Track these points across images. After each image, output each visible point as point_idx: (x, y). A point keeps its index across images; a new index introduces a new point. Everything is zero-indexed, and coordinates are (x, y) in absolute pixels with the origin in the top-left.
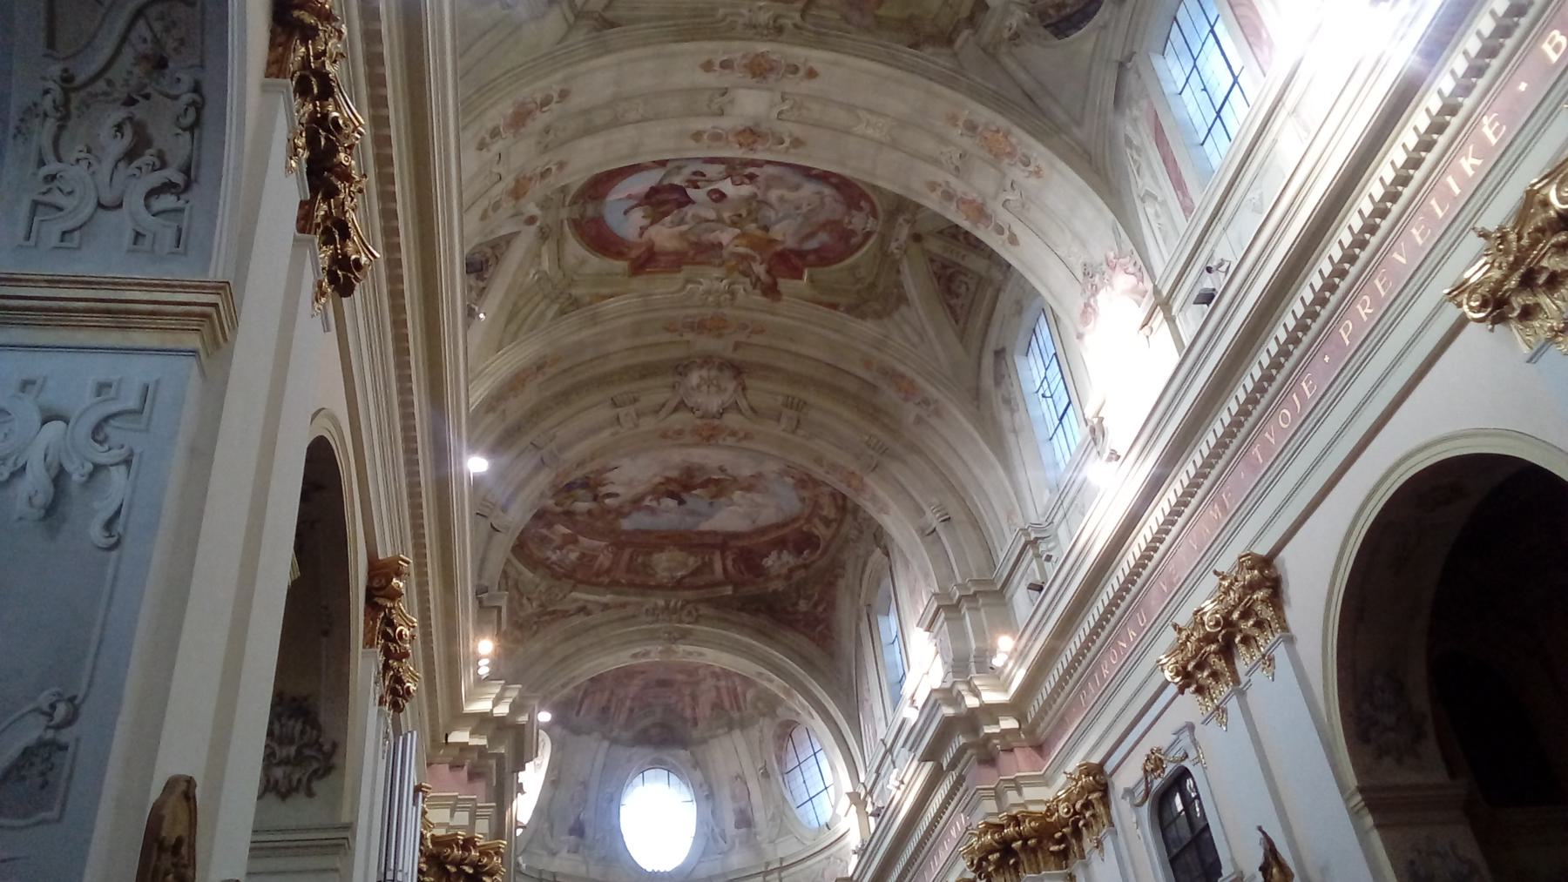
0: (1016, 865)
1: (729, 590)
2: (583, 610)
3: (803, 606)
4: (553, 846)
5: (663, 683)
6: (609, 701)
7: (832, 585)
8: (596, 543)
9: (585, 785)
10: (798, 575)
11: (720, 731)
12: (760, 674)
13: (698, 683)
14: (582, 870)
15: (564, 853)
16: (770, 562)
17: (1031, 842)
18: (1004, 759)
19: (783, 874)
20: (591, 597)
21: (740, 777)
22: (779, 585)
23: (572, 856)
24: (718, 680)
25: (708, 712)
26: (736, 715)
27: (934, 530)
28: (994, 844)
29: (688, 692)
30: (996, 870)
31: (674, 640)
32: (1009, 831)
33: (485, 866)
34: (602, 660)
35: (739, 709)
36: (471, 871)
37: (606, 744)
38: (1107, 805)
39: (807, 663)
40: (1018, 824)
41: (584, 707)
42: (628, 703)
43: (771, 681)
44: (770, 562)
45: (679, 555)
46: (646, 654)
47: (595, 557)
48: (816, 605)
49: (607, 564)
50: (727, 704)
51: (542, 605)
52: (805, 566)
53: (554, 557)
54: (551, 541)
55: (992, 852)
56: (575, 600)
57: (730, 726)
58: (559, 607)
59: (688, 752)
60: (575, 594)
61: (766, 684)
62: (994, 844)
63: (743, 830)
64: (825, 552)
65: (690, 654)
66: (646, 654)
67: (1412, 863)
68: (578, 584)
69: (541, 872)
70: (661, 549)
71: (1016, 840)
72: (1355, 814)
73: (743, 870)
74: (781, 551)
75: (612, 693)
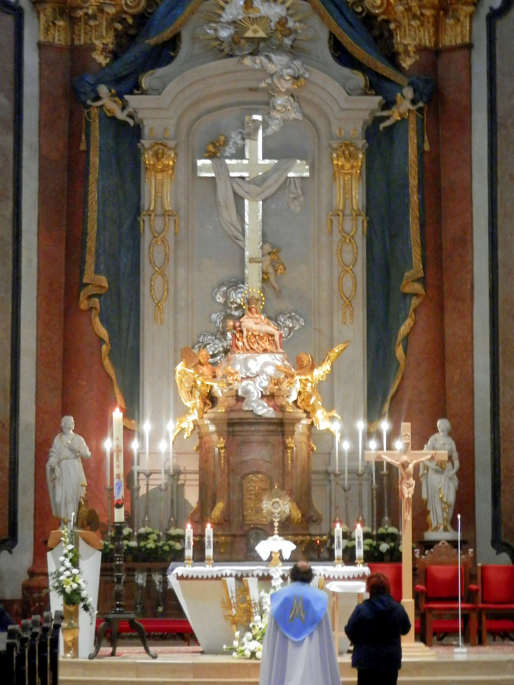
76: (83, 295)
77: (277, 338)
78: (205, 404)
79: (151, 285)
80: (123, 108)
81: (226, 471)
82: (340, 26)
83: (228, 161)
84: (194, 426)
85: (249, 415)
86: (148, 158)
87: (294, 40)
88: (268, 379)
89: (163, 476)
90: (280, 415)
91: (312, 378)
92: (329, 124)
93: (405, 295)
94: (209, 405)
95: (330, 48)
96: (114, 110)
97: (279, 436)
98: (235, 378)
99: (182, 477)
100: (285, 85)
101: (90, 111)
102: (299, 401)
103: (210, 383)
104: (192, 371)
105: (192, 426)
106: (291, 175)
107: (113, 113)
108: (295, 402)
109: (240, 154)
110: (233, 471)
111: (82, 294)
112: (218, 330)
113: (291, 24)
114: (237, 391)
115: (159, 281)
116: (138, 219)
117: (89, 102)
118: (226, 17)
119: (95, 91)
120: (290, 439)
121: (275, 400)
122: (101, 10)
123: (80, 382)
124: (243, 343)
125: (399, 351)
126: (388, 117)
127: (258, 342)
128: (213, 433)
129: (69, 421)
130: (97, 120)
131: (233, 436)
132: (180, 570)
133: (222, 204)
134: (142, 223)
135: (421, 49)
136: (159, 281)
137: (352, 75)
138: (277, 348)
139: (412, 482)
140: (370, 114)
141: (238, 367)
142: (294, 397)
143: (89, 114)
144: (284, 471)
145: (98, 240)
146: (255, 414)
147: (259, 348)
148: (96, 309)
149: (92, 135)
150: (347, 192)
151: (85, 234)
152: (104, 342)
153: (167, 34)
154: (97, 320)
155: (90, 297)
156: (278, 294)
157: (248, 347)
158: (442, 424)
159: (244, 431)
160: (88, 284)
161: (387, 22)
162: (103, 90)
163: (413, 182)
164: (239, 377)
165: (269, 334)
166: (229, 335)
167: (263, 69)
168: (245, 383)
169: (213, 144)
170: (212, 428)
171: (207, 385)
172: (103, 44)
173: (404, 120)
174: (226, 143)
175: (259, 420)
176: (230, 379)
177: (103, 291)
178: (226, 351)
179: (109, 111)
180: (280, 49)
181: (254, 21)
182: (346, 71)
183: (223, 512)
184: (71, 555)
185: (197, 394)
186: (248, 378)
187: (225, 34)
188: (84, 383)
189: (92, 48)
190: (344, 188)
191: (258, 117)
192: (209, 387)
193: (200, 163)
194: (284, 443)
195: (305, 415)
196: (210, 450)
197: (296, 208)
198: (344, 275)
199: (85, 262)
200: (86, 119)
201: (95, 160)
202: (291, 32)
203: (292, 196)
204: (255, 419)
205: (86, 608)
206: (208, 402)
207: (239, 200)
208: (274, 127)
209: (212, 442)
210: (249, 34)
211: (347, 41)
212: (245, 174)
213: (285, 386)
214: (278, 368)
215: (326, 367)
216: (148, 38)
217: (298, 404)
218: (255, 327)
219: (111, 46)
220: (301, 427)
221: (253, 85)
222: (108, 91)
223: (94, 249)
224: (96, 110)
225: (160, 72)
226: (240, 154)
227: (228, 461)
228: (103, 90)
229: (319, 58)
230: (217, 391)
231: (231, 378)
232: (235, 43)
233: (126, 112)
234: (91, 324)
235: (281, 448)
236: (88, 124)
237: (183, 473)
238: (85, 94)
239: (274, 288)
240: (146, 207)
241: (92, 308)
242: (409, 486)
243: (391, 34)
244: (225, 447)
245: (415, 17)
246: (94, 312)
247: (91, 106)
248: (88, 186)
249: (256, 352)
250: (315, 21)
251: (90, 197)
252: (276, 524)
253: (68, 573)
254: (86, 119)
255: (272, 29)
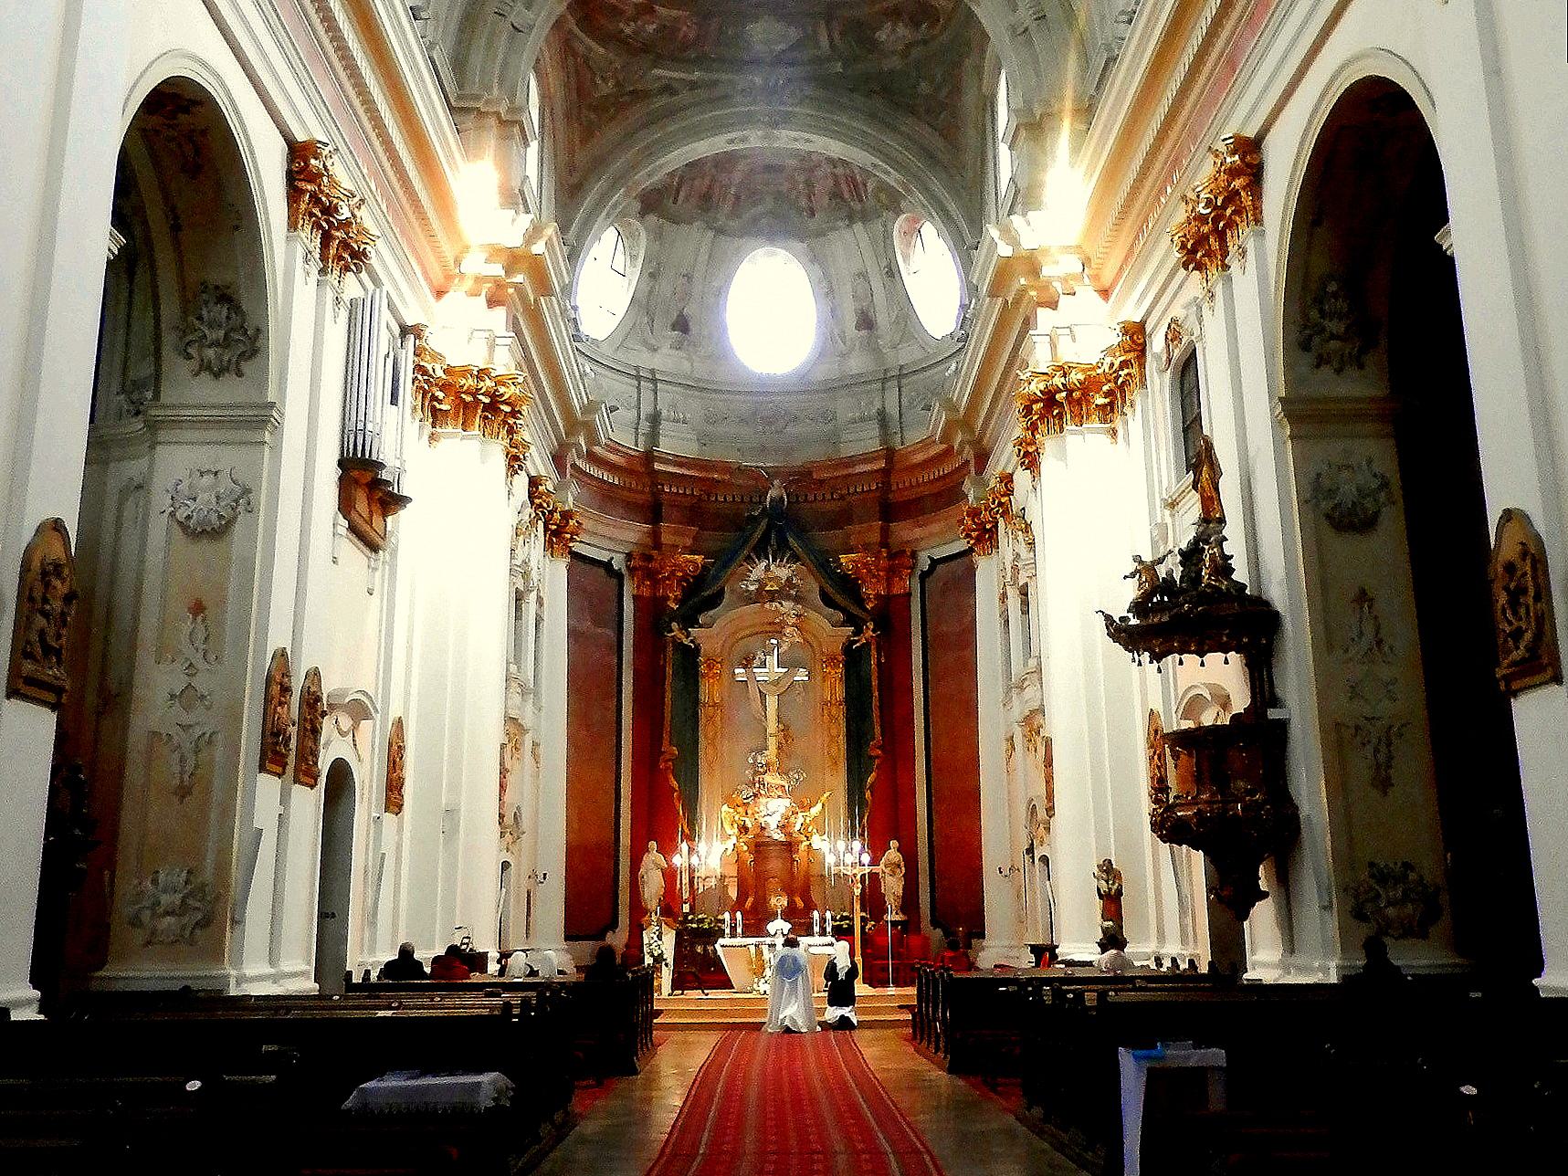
0: (1060, 416)
1: (839, 67)
2: (668, 89)
3: (924, 87)
4: (653, 342)
5: (769, 168)
6: (710, 187)
7: (957, 64)
8: (675, 13)
9: (689, 277)
10: (916, 53)
11: (840, 223)
12: (875, 166)
13: (812, 170)
14: (686, 366)
15: (665, 350)
16: (882, 35)
17: (1076, 395)
18: (1064, 301)
19: (904, 381)
20: (676, 75)
21: (863, 275)
22: (895, 63)
23: (673, 352)
24: (835, 167)
25: (826, 200)
26: (858, 207)
27: (1026, 29)
28: (1039, 394)
29: (801, 178)
30: (1041, 418)
31: (775, 125)
32: (1058, 381)
33: (502, 395)
34: (696, 144)
35: (861, 201)
36: (487, 400)
37: (711, 234)
38: (1142, 366)
39: (930, 157)
40: (1065, 375)
41: (682, 194)
42: (733, 191)
43: (888, 173)
44: (882, 35)
45: (779, 27)
46: (744, 139)
47: (675, 30)
48: (938, 88)
49: (692, 35)
50: (847, 196)
51: (618, 84)
52: (925, 42)
53: (628, 31)
54: (622, 12)
55: (1037, 401)
56: (659, 78)
57: (851, 218)
58: (640, 87)
59: (805, 245)
60: (657, 72)
61: (883, 176)
62: (1039, 394)
63: (864, 333)
64: (945, 28)
65: (796, 140)
66: (744, 139)
67: (1319, 475)
68: (658, 61)
69: (637, 368)
70: (756, 18)
71: (1061, 391)
72: (1276, 424)
73: (860, 375)
74: (895, 24)
75: (713, 180)
77: (787, 788)
78: (741, 833)
83: (755, 670)
86: (703, 669)
89: (713, 879)
92: (820, 645)
93: (870, 757)
99: (726, 880)
100: (792, 621)
104: (732, 810)
106: (796, 679)
109: (763, 665)
115: (710, 751)
118: (753, 577)
122: (673, 573)
125: (868, 794)
126: (857, 641)
128: (745, 852)
129: (653, 845)
132: (721, 941)
135: (878, 596)
136: (710, 751)
139: (860, 885)
141: (762, 808)
142: (798, 827)
150: (833, 688)
153: (715, 588)
156: (789, 757)
158: (894, 844)
161: (858, 579)
162: (674, 625)
163: (875, 683)
164: (762, 814)
166: (757, 785)
167: (777, 610)
168: (766, 818)
169: (745, 659)
170: (745, 848)
173: (868, 644)
174: (754, 658)
175: (777, 843)
176: (756, 816)
178: (755, 795)
180: (788, 597)
181: (770, 579)
183: (753, 904)
184: (657, 933)
185: (736, 826)
187: (752, 588)
189: (668, 598)
191: (774, 641)
193: (737, 671)
196: (744, 862)
197: (799, 700)
201: (669, 671)
202: (794, 586)
205: (666, 965)
207: (763, 696)
208: (785, 647)
210: (767, 588)
211: (830, 590)
212: (766, 679)
213: (792, 820)
215: (819, 806)
220: (803, 847)
221: (771, 620)
225: (711, 613)
226: (763, 665)
228: (674, 625)
234: (667, 780)
242: (858, 888)
243: (859, 587)
245: (874, 576)
250: (811, 579)
252: (779, 912)
253: (655, 944)
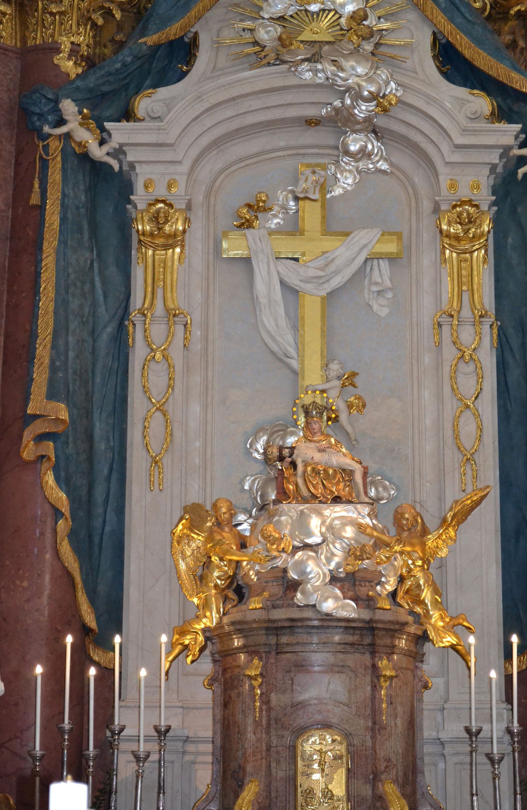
76: (28, 434)
77: (358, 477)
78: (226, 599)
79: (145, 427)
80: (102, 143)
81: (264, 722)
82: (451, 20)
84: (207, 639)
85: (308, 614)
87: (377, 45)
88: (343, 548)
90: (366, 615)
91: (424, 551)
94: (234, 600)
95: (435, 57)
96: (87, 142)
97: (364, 653)
98: (282, 546)
101: (48, 144)
102: (400, 594)
103: (235, 558)
105: (201, 638)
107: (85, 147)
108: (394, 594)
110: (277, 721)
111: (26, 433)
112: (253, 504)
113: (371, 21)
114: (285, 571)
116: (126, 323)
117: (46, 129)
119: (57, 111)
120: (385, 662)
121: (357, 588)
123: (18, 582)
124: (297, 485)
127: (323, 484)
128: (239, 649)
130: (59, 159)
131: (278, 653)
133: (263, 300)
134: (131, 328)
137: (472, 98)
138: (358, 496)
140: (501, 157)
143: (46, 148)
144: (374, 723)
145: (54, 346)
146: (319, 612)
147: (326, 495)
148: (49, 459)
149: (50, 181)
151: (33, 336)
152: (63, 514)
154: (50, 479)
155: (41, 438)
157: (304, 492)
159: (298, 643)
160: (35, 417)
164: (288, 543)
165: (344, 470)
168: (299, 555)
171: (230, 561)
172: (72, 43)
177: (60, 428)
179: (80, 144)
182: (462, 92)
186: (307, 547)
188: (25, 584)
190: (460, 275)
192: (234, 565)
194: (374, 666)
195: (410, 619)
198: (461, 412)
199: (32, 380)
200: (41, 157)
203: (374, 288)
204: (320, 620)
206: (231, 594)
209: (239, 666)
214: (360, 528)
216: (143, 35)
217: (398, 600)
218: (318, 457)
219: (84, 50)
222: (76, 109)
223: (47, 361)
224: (57, 143)
225: (163, 92)
227: (266, 701)
229: (416, 73)
230: (247, 575)
231: (275, 546)
232: (284, 46)
233: (106, 148)
235: (368, 679)
236: (45, 164)
237: (193, 742)
238: (40, 115)
239: (347, 433)
240: (139, 305)
241: (43, 457)
244: (261, 674)
246: (45, 465)
247: (50, 135)
248: (41, 260)
249: (321, 502)
251: (44, 277)
254: (41, 157)
255: (342, 29)
